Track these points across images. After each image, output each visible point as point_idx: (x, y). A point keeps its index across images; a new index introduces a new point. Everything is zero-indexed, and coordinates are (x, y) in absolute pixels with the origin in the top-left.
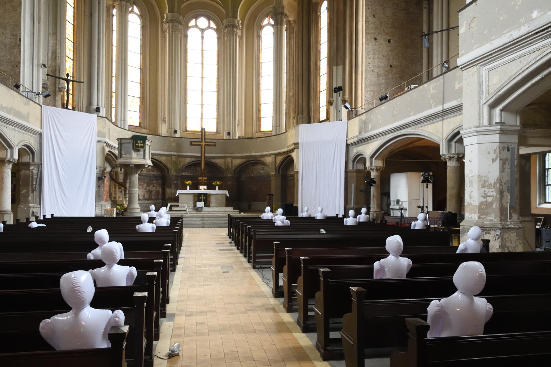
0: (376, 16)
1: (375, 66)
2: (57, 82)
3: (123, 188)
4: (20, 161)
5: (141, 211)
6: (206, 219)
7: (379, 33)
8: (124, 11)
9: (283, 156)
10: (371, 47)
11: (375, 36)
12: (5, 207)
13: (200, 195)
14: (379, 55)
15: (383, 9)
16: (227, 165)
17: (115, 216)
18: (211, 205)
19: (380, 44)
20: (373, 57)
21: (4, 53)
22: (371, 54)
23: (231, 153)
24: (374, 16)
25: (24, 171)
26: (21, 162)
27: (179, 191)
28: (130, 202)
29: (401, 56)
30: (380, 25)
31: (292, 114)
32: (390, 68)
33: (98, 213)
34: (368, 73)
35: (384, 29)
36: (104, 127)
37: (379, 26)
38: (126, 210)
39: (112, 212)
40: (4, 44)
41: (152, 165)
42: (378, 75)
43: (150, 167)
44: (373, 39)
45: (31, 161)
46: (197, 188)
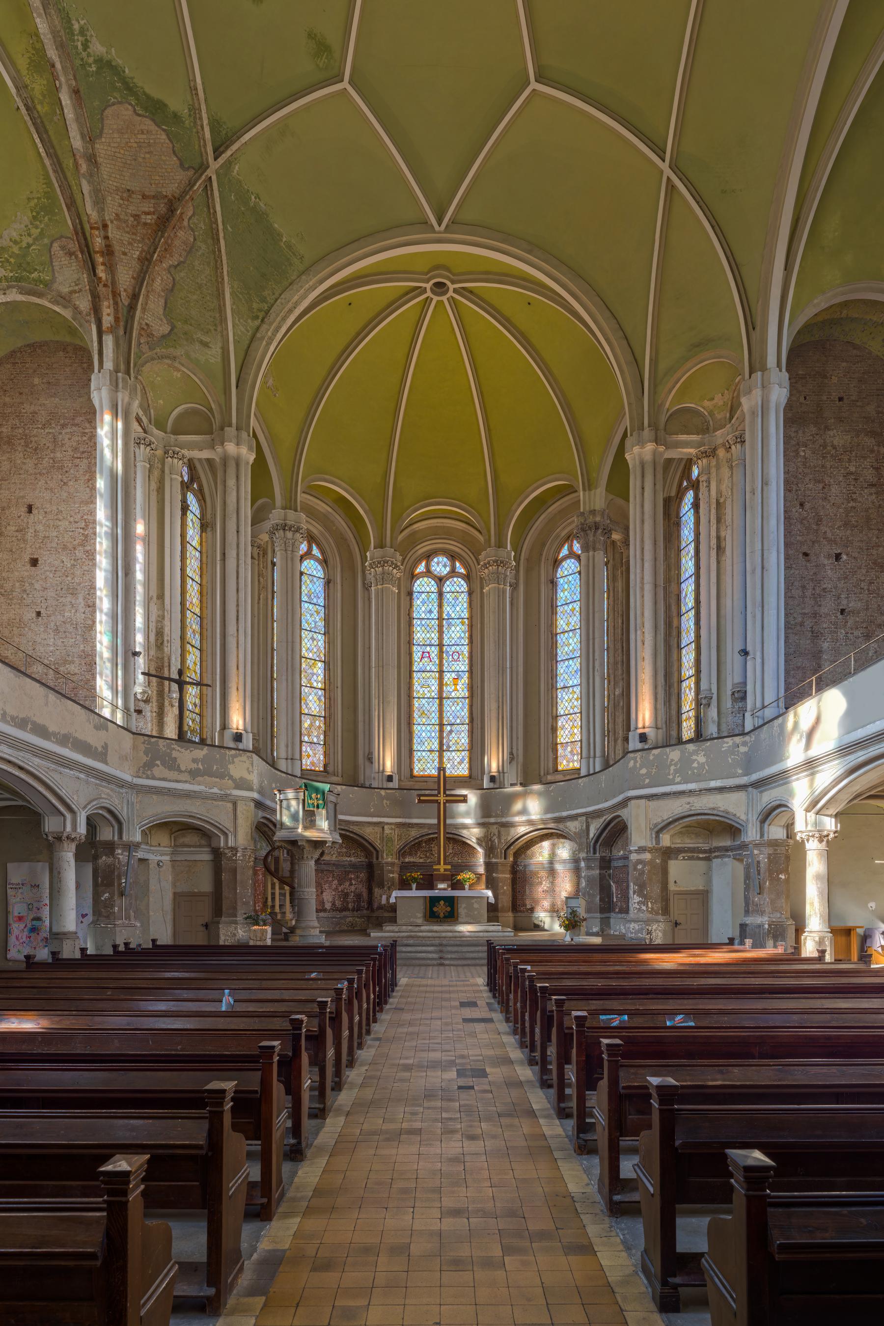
0: (807, 506)
1: (805, 614)
2: (167, 689)
3: (287, 888)
4: (98, 839)
5: (321, 932)
6: (449, 949)
7: (813, 542)
8: (290, 549)
9: (602, 820)
10: (797, 572)
11: (805, 549)
12: (64, 926)
13: (434, 900)
14: (814, 589)
15: (824, 488)
16: (490, 839)
17: (269, 942)
18: (460, 920)
19: (816, 566)
20: (801, 593)
21: (74, 640)
22: (797, 589)
23: (497, 816)
24: (802, 505)
25: (104, 858)
26: (100, 841)
27: (395, 894)
28: (299, 914)
29: (866, 588)
30: (817, 525)
31: (621, 732)
32: (840, 617)
33: (242, 935)
34: (790, 631)
35: (825, 532)
36: (250, 769)
37: (815, 527)
38: (292, 930)
39: (263, 934)
40: (72, 624)
41: (341, 841)
42: (812, 632)
43: (337, 846)
44: (801, 555)
45: (116, 838)
46: (431, 887)
